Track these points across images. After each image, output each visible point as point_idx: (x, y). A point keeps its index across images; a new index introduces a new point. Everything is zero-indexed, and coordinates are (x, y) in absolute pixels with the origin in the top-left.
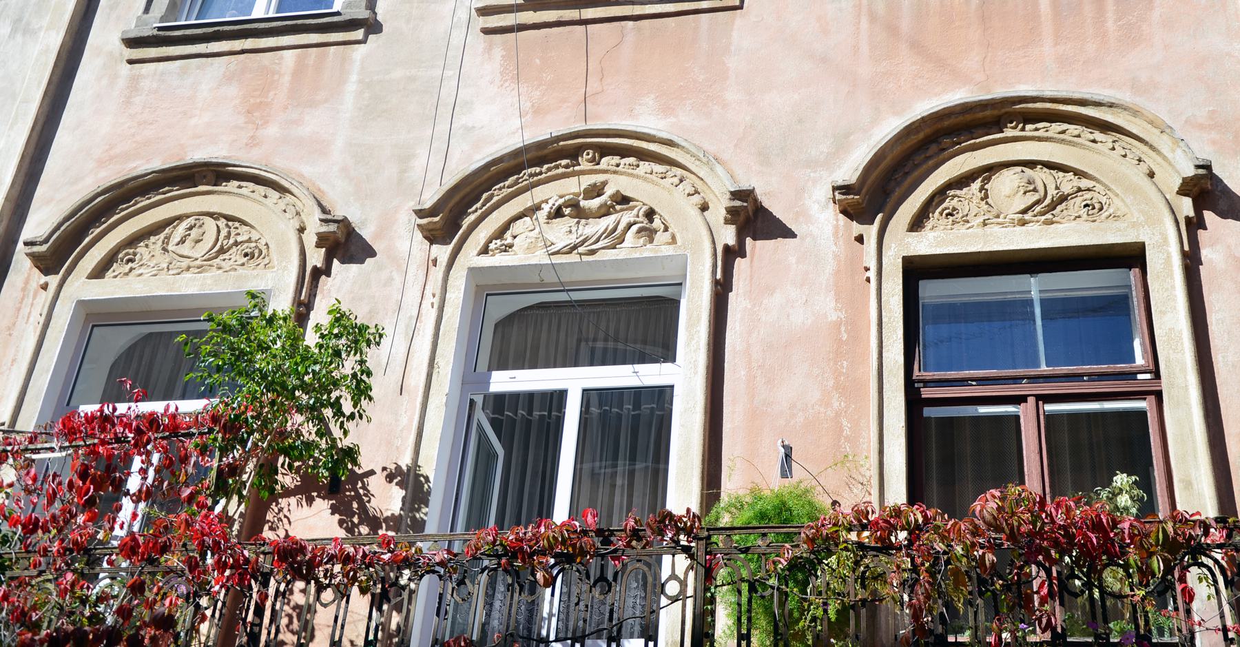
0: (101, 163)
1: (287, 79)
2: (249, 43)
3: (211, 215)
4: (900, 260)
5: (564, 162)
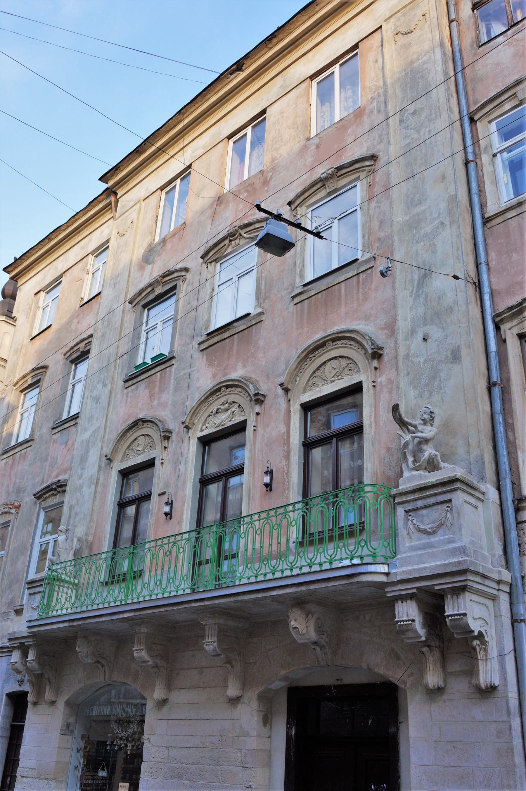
0: (122, 425)
1: (158, 383)
2: (149, 373)
3: (143, 435)
4: (299, 406)
5: (217, 394)
